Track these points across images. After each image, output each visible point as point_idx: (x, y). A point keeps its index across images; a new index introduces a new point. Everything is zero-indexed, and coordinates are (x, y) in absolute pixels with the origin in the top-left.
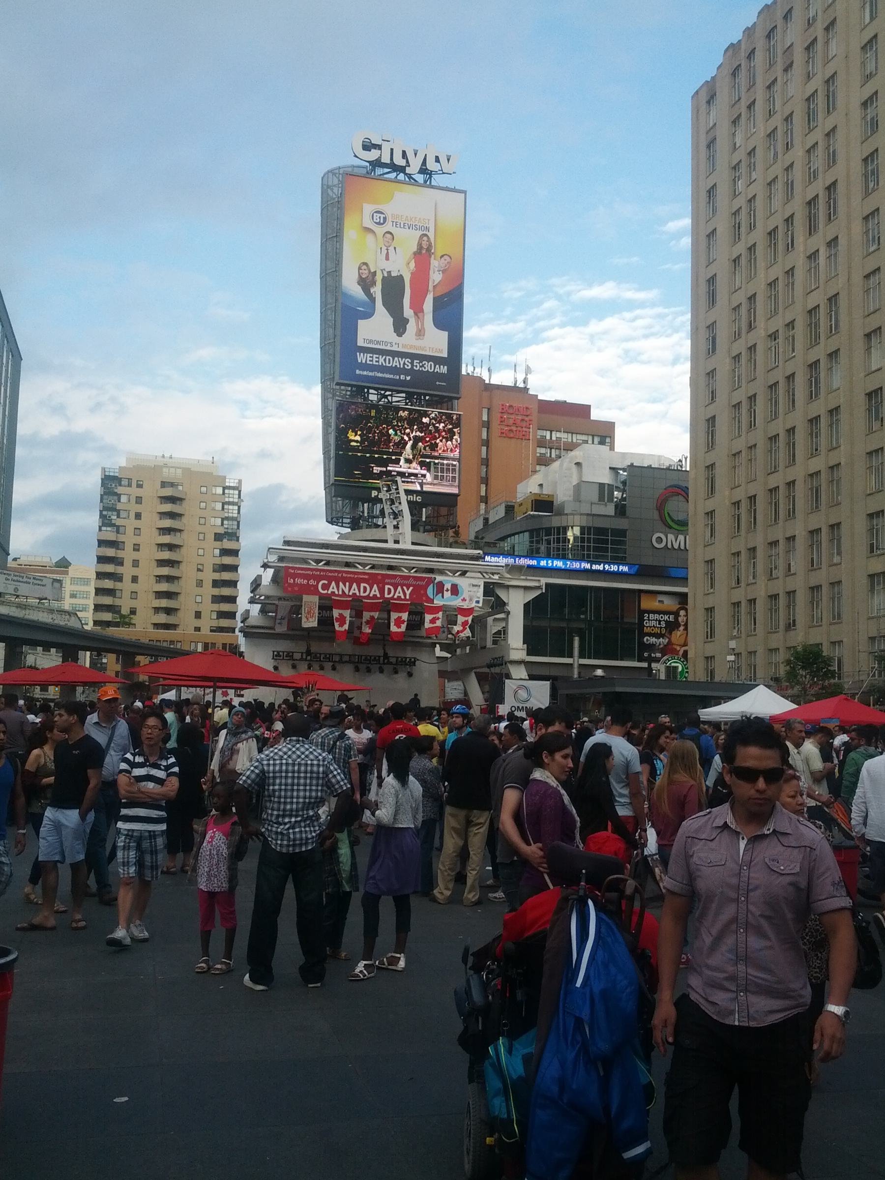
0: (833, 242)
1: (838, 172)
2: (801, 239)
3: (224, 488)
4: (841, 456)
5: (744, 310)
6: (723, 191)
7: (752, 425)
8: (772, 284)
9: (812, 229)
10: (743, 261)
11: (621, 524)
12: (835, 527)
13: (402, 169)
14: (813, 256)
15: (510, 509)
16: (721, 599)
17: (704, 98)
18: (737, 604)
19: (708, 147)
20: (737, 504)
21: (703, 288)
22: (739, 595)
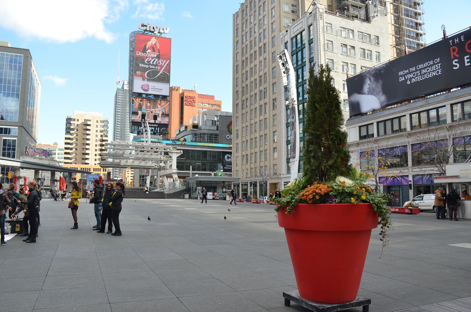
9: (260, 55)
11: (217, 132)
13: (153, 32)
15: (186, 127)
17: (235, 15)
18: (243, 156)
22: (244, 153)
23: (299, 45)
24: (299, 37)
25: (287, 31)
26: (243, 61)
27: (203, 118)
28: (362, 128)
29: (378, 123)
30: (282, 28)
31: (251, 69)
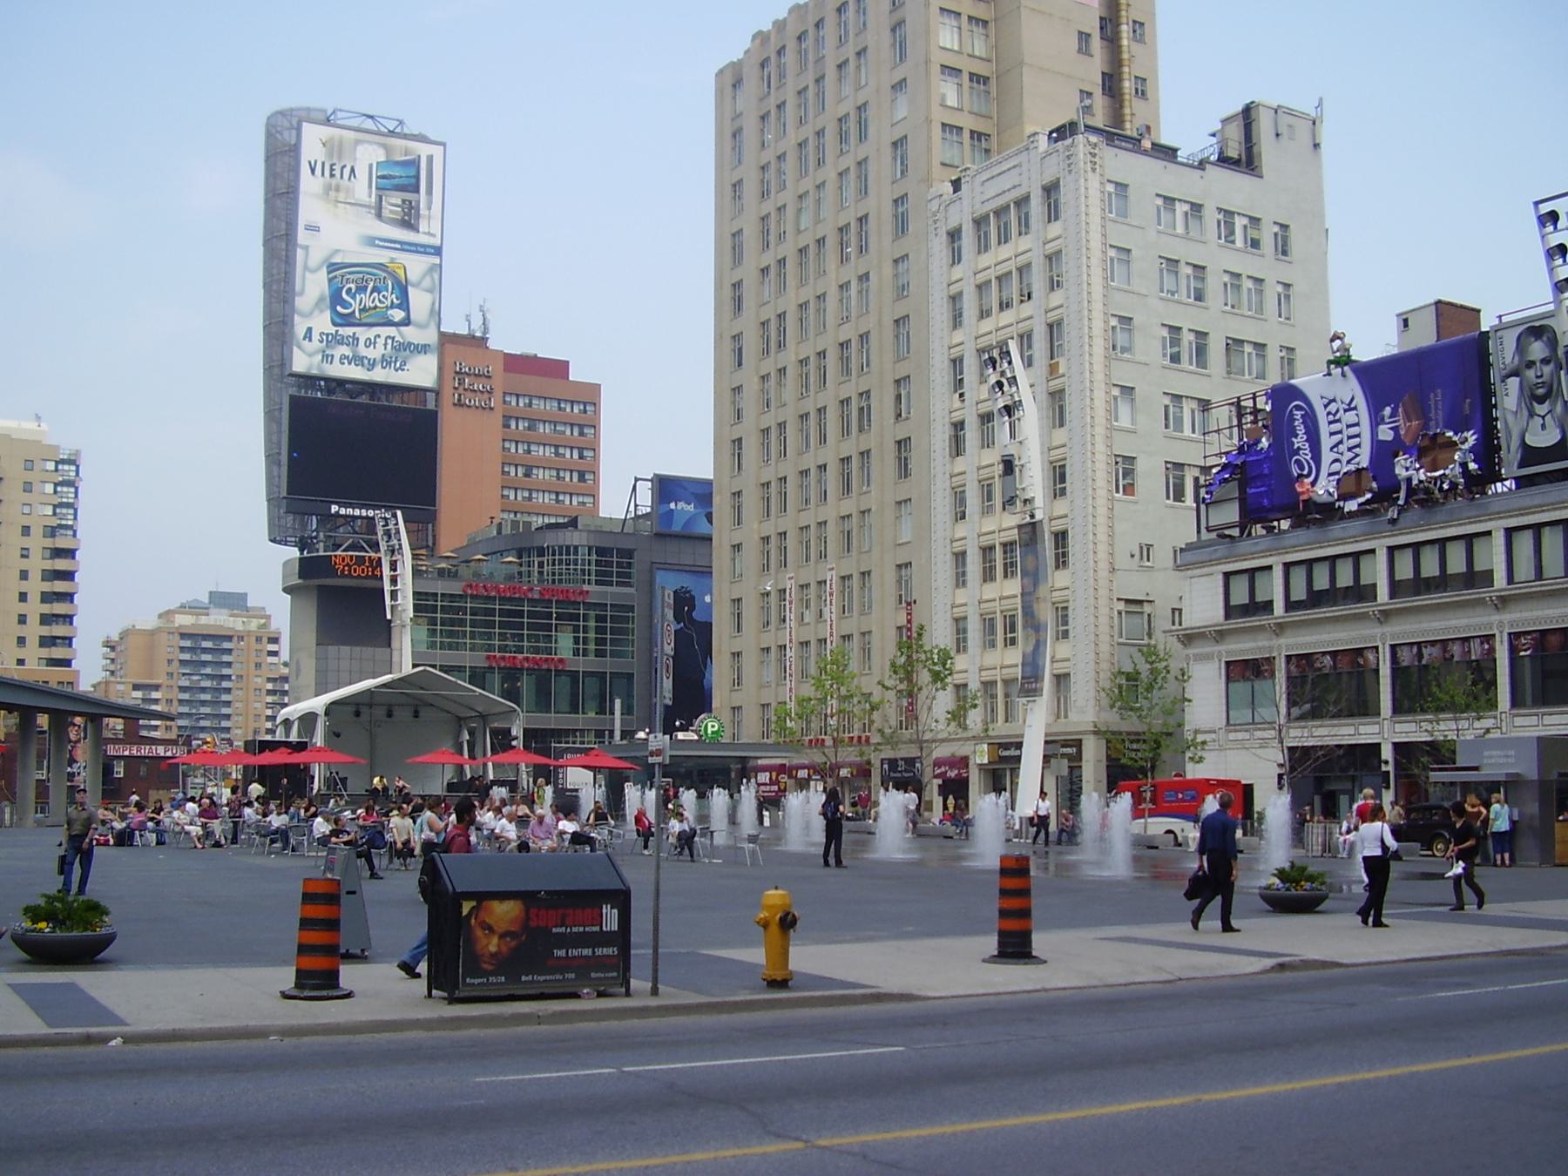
0: (864, 278)
1: (870, 205)
2: (833, 267)
3: (57, 463)
4: (871, 501)
5: (773, 326)
6: (750, 190)
8: (803, 306)
10: (773, 271)
12: (865, 574)
14: (844, 287)
16: (749, 642)
17: (729, 80)
19: (734, 136)
20: (766, 540)
21: (728, 292)
25: (956, 184)
28: (1234, 581)
30: (937, 170)
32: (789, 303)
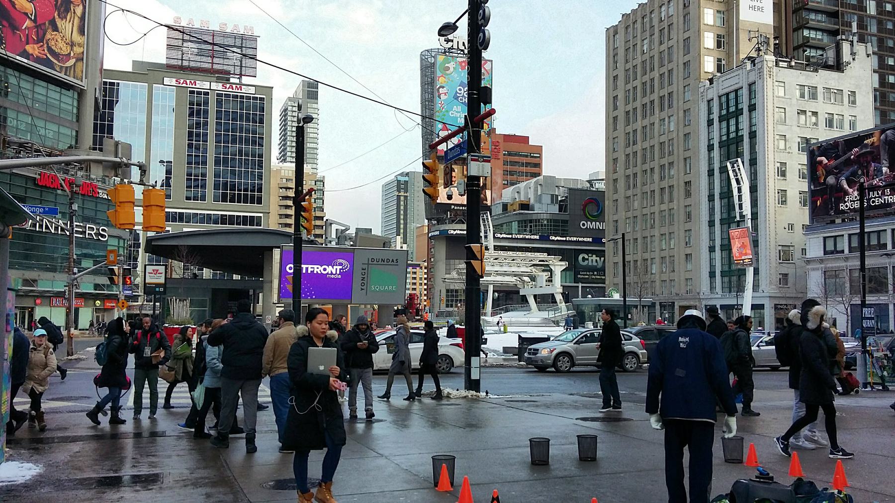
6: (621, 82)
7: (635, 186)
11: (565, 216)
17: (612, 31)
23: (732, 109)
24: (732, 96)
26: (627, 113)
27: (536, 190)
29: (850, 235)
31: (644, 127)
32: (639, 125)
